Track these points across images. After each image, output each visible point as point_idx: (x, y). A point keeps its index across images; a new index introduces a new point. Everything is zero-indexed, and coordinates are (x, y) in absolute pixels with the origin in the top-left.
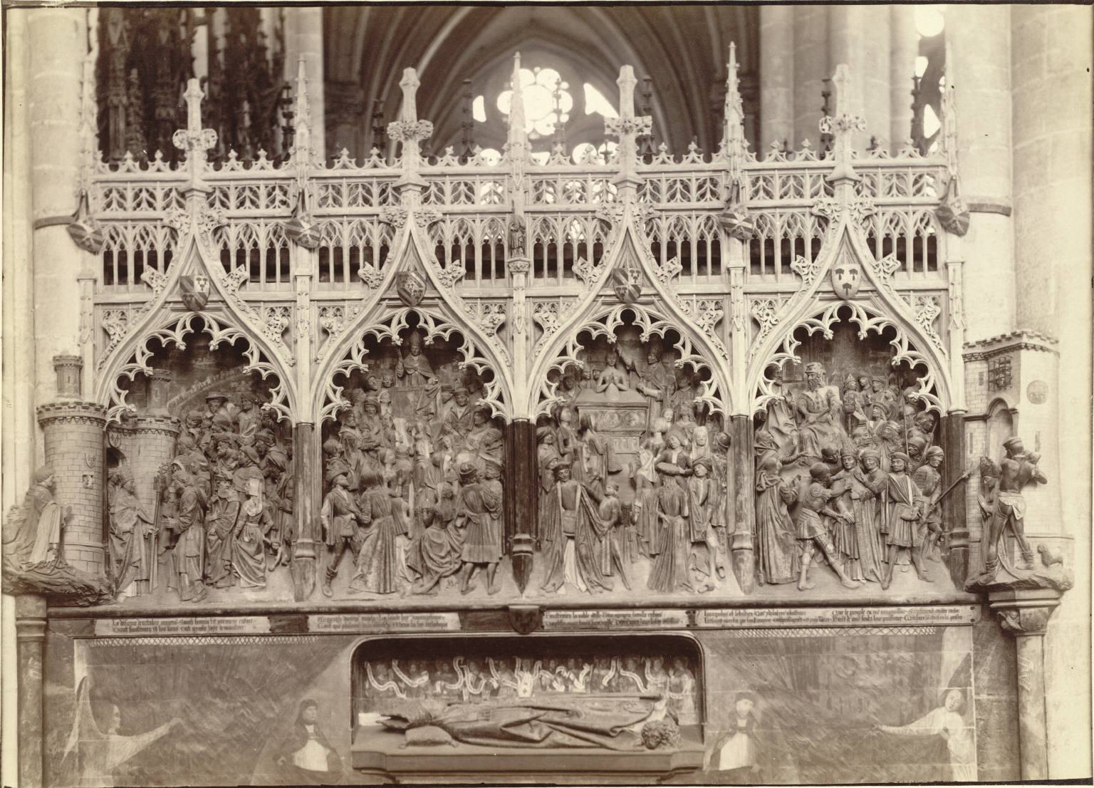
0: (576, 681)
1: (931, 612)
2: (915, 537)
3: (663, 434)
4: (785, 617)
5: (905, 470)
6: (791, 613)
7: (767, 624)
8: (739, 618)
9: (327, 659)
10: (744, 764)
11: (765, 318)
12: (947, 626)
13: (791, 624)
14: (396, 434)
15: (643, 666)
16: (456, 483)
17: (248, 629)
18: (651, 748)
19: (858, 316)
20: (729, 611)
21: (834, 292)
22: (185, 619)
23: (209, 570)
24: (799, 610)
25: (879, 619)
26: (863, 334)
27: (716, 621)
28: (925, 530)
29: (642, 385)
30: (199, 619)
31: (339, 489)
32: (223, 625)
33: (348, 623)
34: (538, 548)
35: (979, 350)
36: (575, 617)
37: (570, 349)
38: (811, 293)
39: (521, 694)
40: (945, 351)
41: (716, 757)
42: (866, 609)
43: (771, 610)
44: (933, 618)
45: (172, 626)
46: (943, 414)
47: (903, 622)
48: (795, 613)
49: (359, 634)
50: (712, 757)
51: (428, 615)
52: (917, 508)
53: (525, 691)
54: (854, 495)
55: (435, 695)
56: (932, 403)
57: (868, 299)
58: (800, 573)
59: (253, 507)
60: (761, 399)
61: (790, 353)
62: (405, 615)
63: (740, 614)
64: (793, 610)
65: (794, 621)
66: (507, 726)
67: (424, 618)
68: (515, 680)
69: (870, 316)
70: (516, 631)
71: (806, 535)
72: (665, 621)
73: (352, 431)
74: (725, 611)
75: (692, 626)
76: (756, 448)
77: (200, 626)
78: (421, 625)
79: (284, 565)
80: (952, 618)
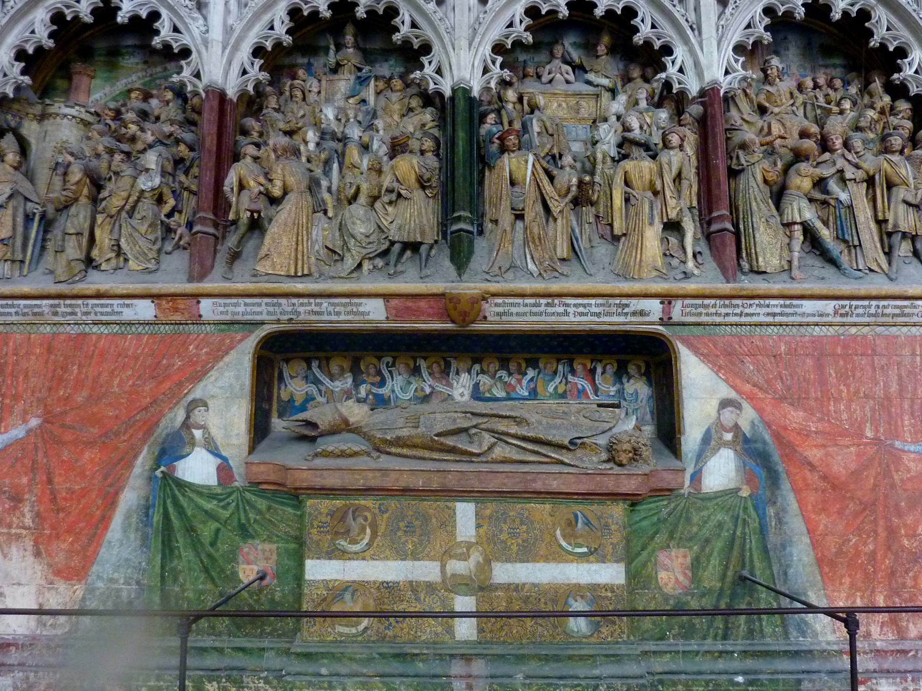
0: (518, 388)
3: (619, 118)
4: (778, 310)
5: (901, 152)
6: (785, 306)
7: (755, 319)
8: (723, 311)
9: (219, 353)
10: (732, 486)
13: (784, 319)
14: (323, 117)
15: (593, 372)
16: (385, 158)
17: (128, 314)
18: (621, 465)
20: (713, 301)
22: (51, 302)
23: (95, 253)
24: (795, 302)
27: (694, 315)
29: (591, 77)
30: (68, 302)
31: (249, 160)
32: (99, 309)
33: (249, 309)
34: (481, 232)
36: (526, 305)
37: (517, 20)
39: (457, 397)
41: (697, 477)
42: (874, 303)
43: (762, 302)
45: (36, 310)
49: (262, 323)
50: (693, 477)
51: (347, 300)
53: (462, 395)
54: (848, 175)
55: (359, 401)
58: (790, 262)
59: (149, 182)
60: (729, 77)
62: (318, 301)
63: (725, 306)
64: (788, 302)
65: (787, 315)
66: (439, 435)
67: (344, 305)
68: (450, 385)
70: (453, 322)
72: (634, 314)
73: (276, 114)
74: (707, 302)
75: (666, 321)
77: (69, 310)
78: (338, 314)
79: (185, 248)
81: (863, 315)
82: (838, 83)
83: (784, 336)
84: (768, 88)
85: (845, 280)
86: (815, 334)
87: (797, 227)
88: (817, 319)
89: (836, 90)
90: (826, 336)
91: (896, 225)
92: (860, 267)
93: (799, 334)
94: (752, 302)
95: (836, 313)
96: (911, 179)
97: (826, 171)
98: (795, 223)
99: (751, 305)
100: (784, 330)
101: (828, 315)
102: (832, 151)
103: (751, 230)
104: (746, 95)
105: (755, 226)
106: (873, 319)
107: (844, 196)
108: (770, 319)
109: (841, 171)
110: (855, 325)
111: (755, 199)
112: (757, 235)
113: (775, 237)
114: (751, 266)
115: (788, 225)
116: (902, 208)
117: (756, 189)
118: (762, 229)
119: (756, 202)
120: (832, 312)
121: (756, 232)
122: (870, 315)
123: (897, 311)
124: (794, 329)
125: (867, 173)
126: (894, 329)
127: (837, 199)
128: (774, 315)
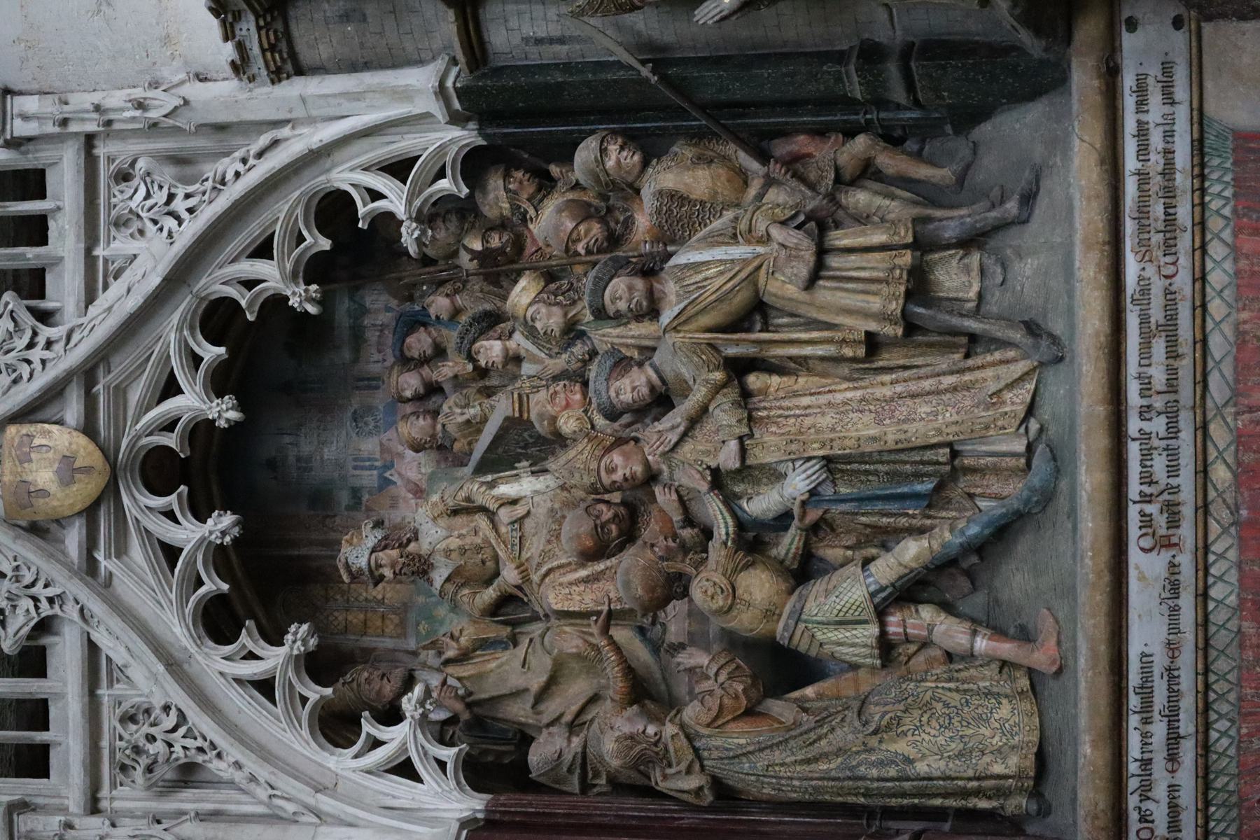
1: (1143, 177)
2: (879, 238)
4: (1159, 729)
5: (649, 270)
6: (1147, 706)
7: (1187, 797)
11: (158, 748)
12: (1200, 118)
13: (1187, 704)
19: (170, 426)
21: (90, 513)
24: (1134, 678)
25: (1172, 373)
26: (225, 411)
28: (860, 198)
35: (248, 27)
38: (76, 589)
40: (264, 140)
42: (1134, 425)
43: (1133, 784)
44: (1168, 171)
46: (465, 137)
47: (1183, 281)
48: (1146, 692)
52: (777, 233)
54: (728, 458)
56: (441, 174)
57: (120, 393)
61: (274, 659)
64: (1134, 701)
65: (1174, 694)
69: (171, 388)
71: (874, 630)
76: (585, 787)
80: (1169, 99)
81: (1172, 453)
82: (419, 342)
83: (1240, 699)
84: (439, 576)
85: (1062, 502)
86: (1232, 600)
87: (894, 623)
88: (1187, 601)
89: (440, 352)
90: (1239, 565)
91: (883, 317)
92: (1020, 446)
93: (1232, 651)
94: (1134, 816)
95: (1166, 543)
96: (738, 251)
97: (723, 526)
98: (883, 633)
99: (1143, 819)
100: (1221, 697)
101: (1173, 566)
102: (652, 477)
103: (907, 785)
104: (463, 657)
105: (892, 772)
106: (1186, 422)
107: (798, 483)
108: (1188, 751)
109: (718, 479)
110: (1203, 471)
111: (808, 761)
112: (922, 768)
113: (927, 707)
114: (1021, 790)
115: (886, 647)
116: (827, 294)
117: (777, 756)
118: (901, 747)
119: (816, 760)
120: (1166, 555)
121: (910, 771)
122: (1173, 431)
123: (1159, 347)
124: (1221, 665)
125: (718, 389)
126: (1217, 344)
127: (804, 503)
128: (1174, 739)
